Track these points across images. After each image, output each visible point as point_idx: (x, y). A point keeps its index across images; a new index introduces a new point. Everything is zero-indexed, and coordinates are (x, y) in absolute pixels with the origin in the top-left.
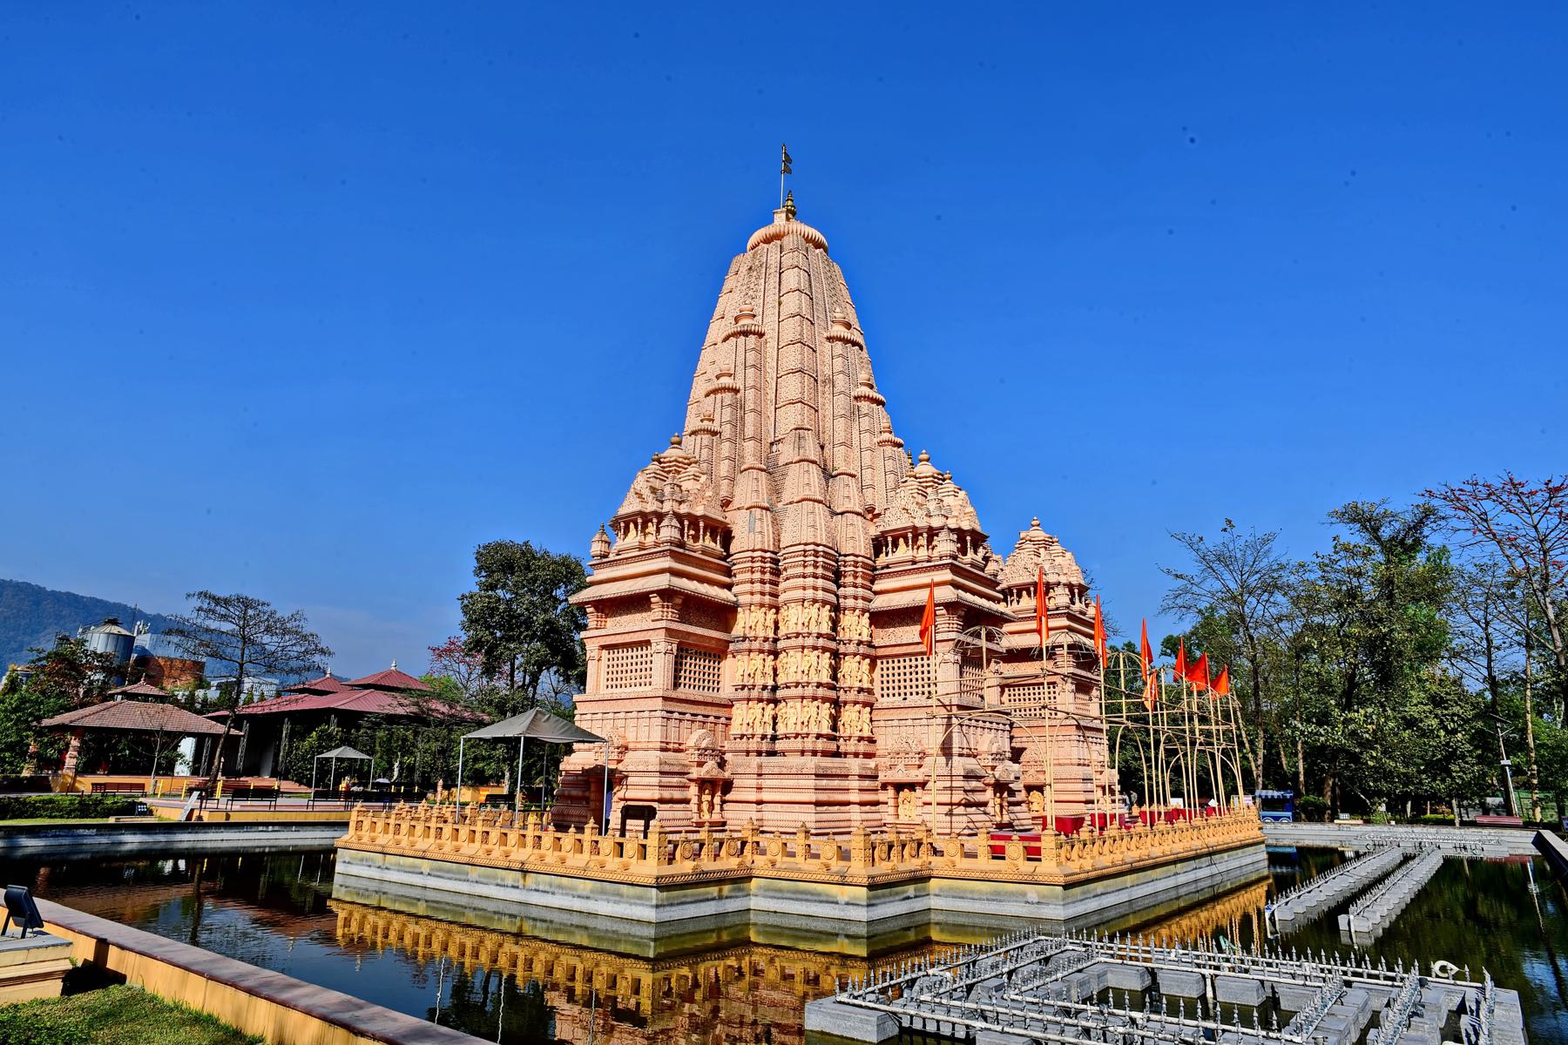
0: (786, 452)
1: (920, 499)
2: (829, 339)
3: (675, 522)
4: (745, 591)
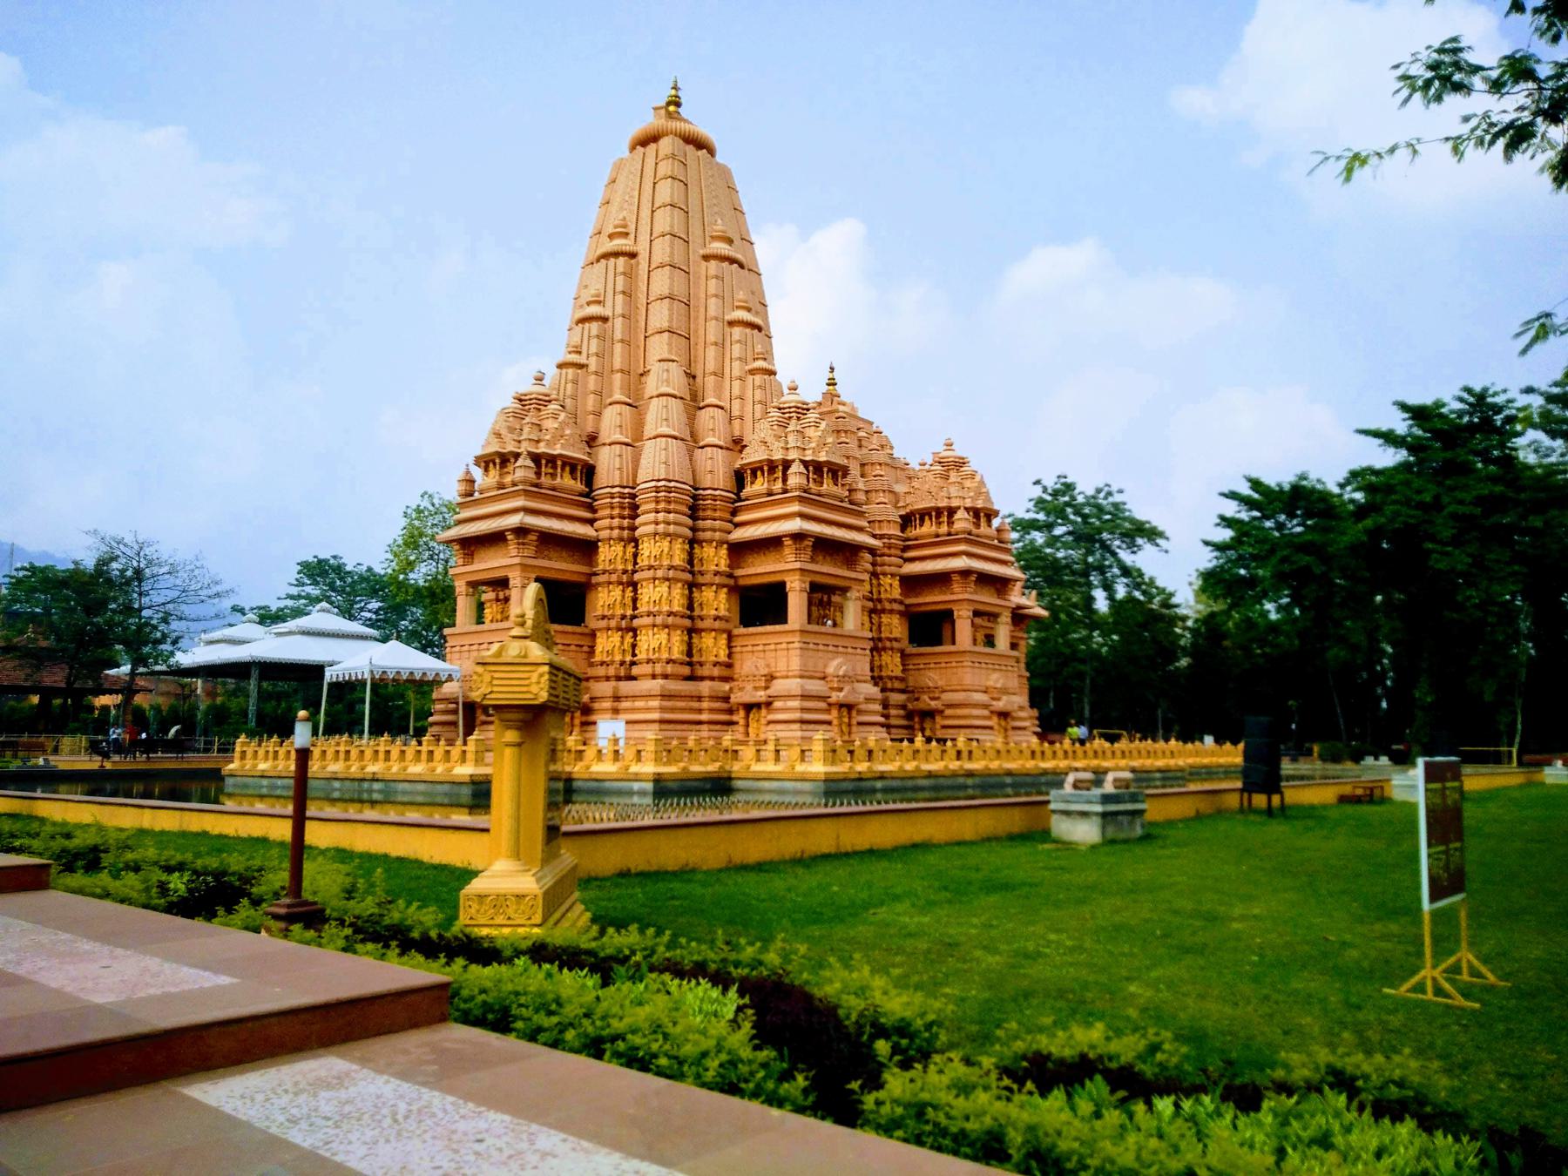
0: (652, 385)
1: (780, 431)
2: (706, 258)
3: (529, 463)
4: (606, 527)
